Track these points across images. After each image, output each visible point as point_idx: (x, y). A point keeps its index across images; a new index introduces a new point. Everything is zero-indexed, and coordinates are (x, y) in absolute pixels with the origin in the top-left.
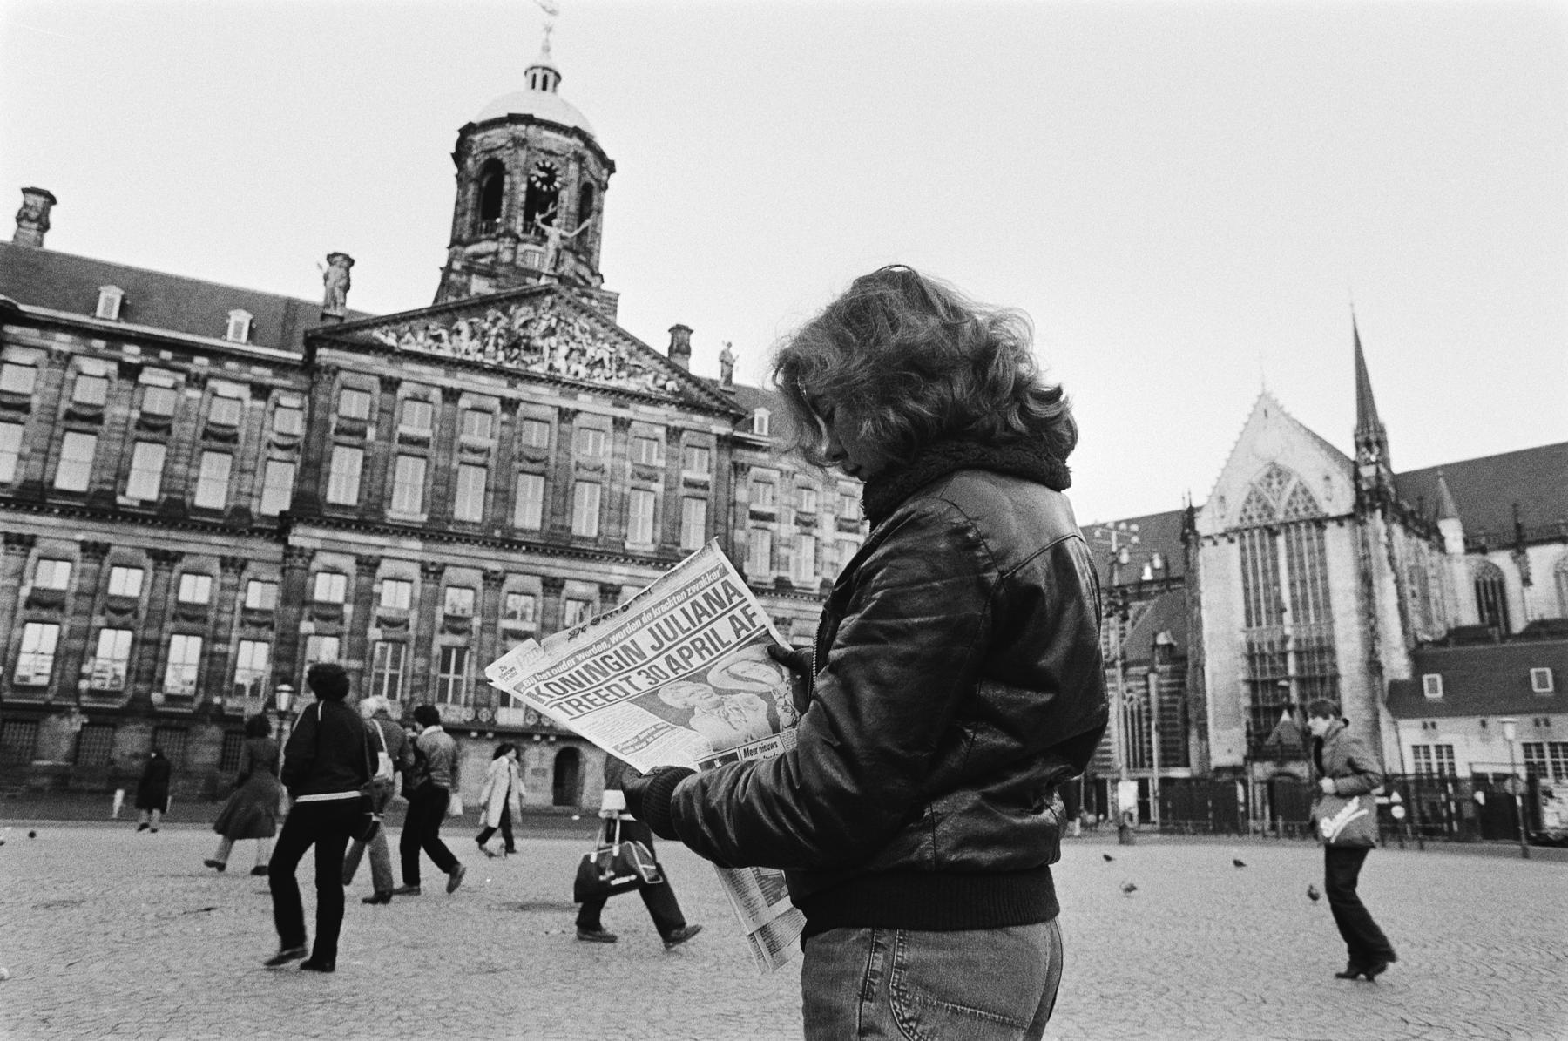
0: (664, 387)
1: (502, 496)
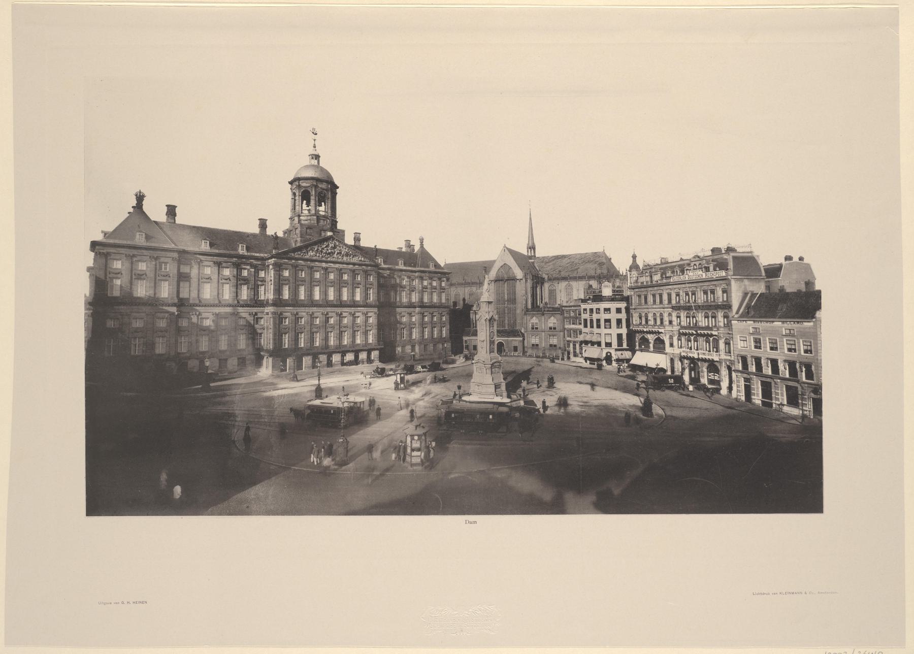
0: (361, 260)
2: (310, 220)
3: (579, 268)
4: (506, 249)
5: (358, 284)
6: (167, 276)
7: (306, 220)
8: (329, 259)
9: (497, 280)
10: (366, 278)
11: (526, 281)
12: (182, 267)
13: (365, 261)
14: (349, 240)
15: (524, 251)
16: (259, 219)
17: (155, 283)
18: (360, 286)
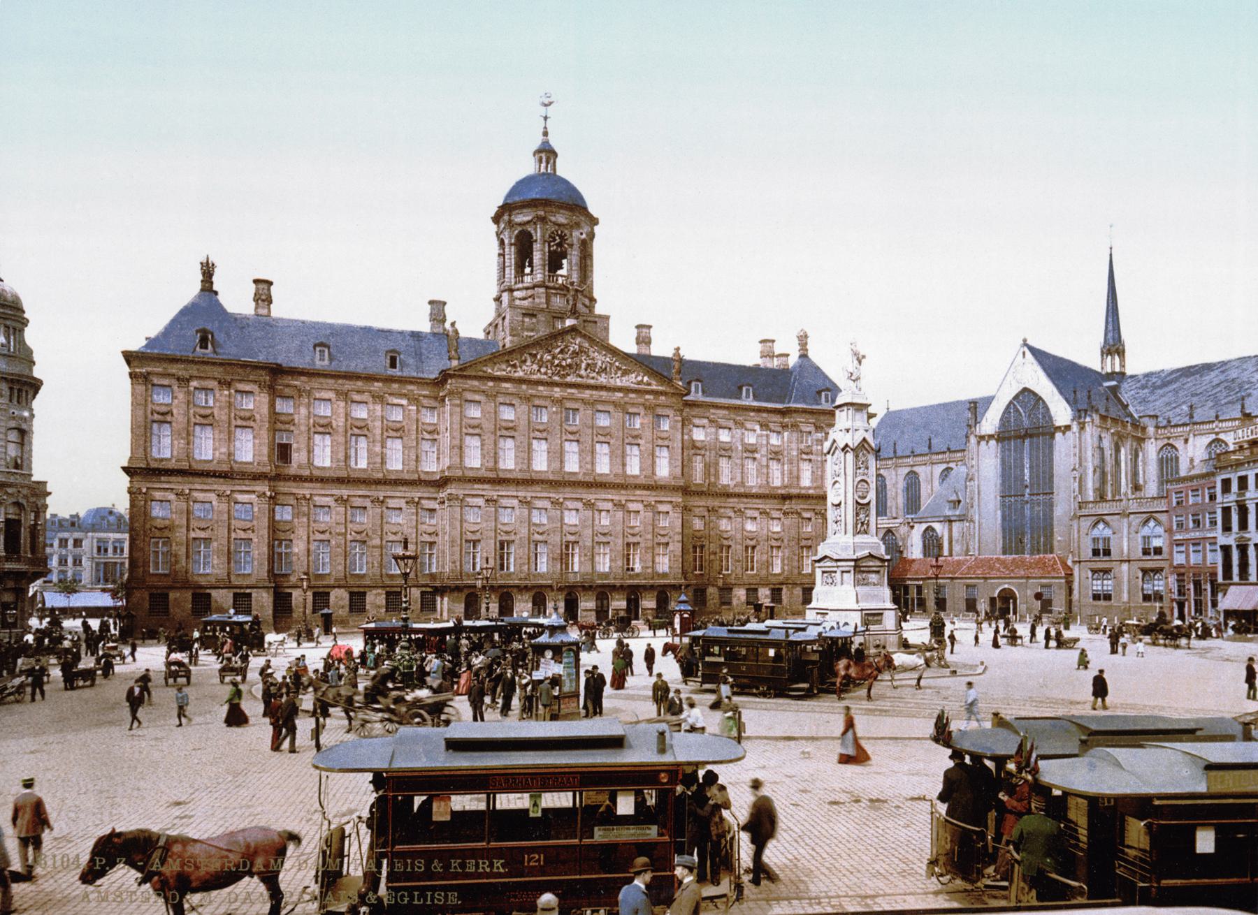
0: (642, 381)
1: (558, 456)
2: (531, 296)
3: (1249, 395)
4: (1026, 349)
5: (636, 437)
6: (249, 419)
7: (524, 299)
8: (569, 379)
9: (1001, 437)
10: (656, 426)
11: (1082, 427)
12: (278, 401)
13: (649, 384)
14: (623, 339)
15: (1088, 355)
16: (431, 302)
17: (230, 433)
18: (640, 441)
